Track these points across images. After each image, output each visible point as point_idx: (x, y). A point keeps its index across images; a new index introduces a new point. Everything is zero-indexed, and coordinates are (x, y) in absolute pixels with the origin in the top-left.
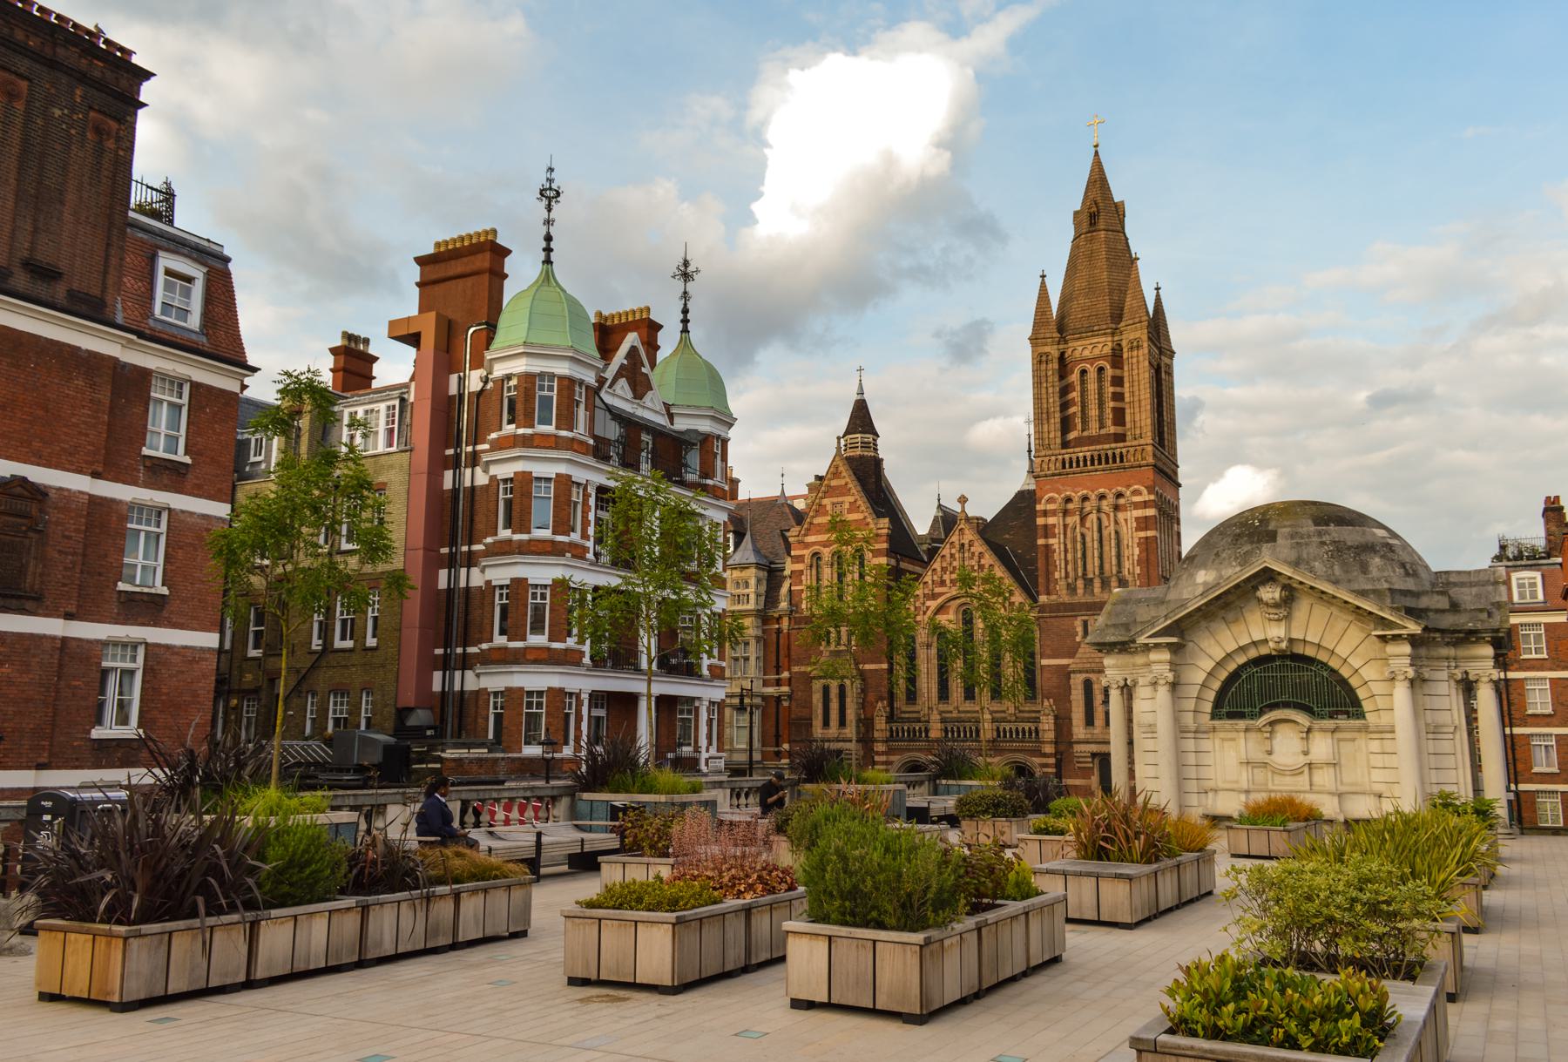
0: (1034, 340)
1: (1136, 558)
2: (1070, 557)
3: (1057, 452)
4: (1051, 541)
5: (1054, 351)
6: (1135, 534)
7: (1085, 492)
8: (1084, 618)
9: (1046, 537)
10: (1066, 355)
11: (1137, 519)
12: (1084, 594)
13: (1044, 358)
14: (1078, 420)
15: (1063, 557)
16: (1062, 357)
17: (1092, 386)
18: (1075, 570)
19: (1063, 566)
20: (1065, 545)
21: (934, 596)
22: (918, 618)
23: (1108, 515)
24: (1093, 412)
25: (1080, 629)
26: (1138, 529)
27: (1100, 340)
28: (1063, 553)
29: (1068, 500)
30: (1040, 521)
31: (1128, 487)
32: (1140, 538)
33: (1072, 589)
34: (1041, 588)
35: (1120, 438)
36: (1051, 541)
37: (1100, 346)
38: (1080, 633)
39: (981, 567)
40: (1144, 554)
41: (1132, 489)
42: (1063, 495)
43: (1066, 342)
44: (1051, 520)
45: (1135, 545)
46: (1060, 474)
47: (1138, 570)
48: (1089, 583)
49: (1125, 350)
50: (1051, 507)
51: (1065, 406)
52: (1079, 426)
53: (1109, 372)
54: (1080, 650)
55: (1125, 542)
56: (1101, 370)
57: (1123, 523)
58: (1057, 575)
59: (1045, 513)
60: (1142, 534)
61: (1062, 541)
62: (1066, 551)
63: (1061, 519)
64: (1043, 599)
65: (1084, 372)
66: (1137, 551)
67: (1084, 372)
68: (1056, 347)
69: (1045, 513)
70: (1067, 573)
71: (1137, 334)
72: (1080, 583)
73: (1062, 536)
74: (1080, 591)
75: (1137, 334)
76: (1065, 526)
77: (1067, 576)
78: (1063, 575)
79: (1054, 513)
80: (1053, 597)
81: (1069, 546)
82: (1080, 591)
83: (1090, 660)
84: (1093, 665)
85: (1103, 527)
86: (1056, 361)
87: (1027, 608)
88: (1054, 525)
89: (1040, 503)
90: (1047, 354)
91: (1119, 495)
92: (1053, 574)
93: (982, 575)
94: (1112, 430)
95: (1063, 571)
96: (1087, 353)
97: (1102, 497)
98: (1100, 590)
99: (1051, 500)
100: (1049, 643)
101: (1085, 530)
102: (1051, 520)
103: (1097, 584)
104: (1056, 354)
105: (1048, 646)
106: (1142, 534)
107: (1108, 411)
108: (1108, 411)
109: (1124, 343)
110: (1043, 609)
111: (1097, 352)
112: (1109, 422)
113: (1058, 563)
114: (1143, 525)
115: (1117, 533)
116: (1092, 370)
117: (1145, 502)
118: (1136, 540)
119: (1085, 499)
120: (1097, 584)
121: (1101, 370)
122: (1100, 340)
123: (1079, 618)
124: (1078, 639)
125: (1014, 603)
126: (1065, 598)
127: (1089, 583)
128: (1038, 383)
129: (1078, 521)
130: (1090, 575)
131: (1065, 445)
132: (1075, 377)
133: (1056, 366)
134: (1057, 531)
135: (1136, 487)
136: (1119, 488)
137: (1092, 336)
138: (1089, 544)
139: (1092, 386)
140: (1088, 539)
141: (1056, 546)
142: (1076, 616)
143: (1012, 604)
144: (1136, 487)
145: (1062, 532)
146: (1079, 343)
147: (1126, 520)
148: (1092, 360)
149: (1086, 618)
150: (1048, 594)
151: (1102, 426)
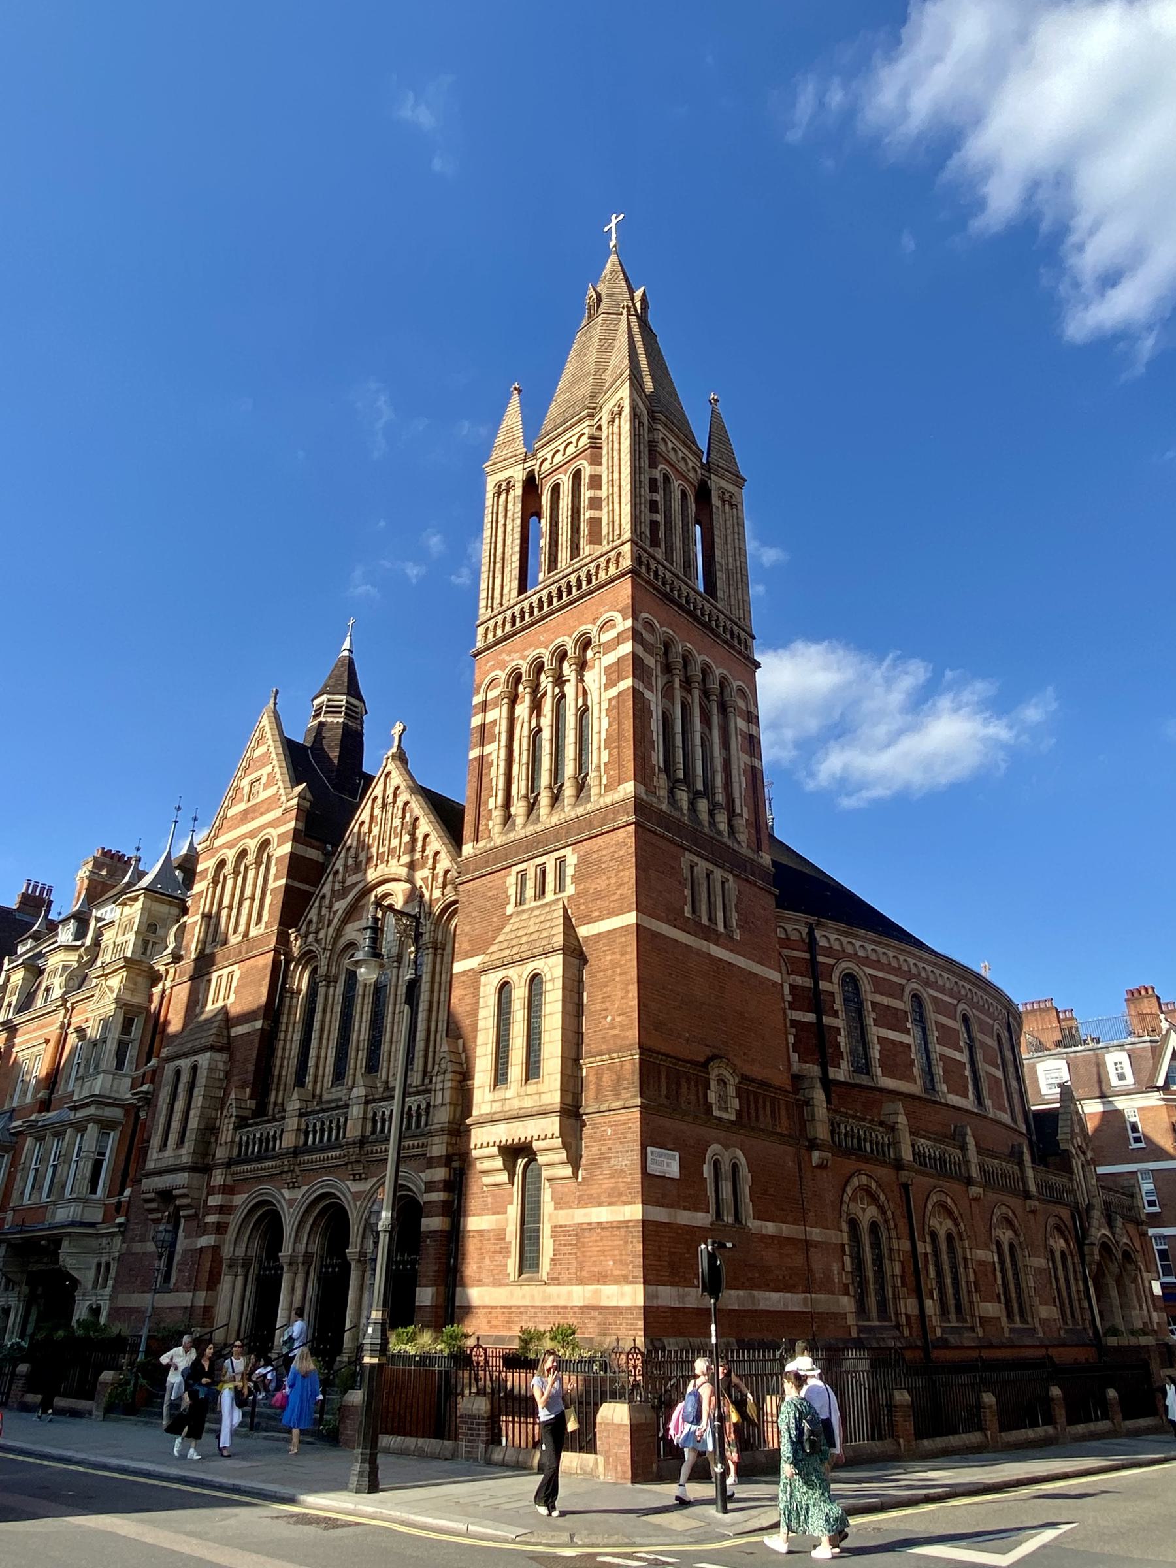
1: (603, 736)
7: (537, 651)
12: (525, 825)
21: (344, 892)
22: (321, 935)
25: (512, 891)
26: (610, 684)
32: (610, 700)
34: (468, 831)
40: (615, 727)
46: (506, 638)
54: (507, 929)
64: (468, 849)
88: (494, 722)
92: (487, 803)
114: (614, 676)
118: (605, 705)
121: (577, 475)
124: (510, 909)
141: (494, 756)
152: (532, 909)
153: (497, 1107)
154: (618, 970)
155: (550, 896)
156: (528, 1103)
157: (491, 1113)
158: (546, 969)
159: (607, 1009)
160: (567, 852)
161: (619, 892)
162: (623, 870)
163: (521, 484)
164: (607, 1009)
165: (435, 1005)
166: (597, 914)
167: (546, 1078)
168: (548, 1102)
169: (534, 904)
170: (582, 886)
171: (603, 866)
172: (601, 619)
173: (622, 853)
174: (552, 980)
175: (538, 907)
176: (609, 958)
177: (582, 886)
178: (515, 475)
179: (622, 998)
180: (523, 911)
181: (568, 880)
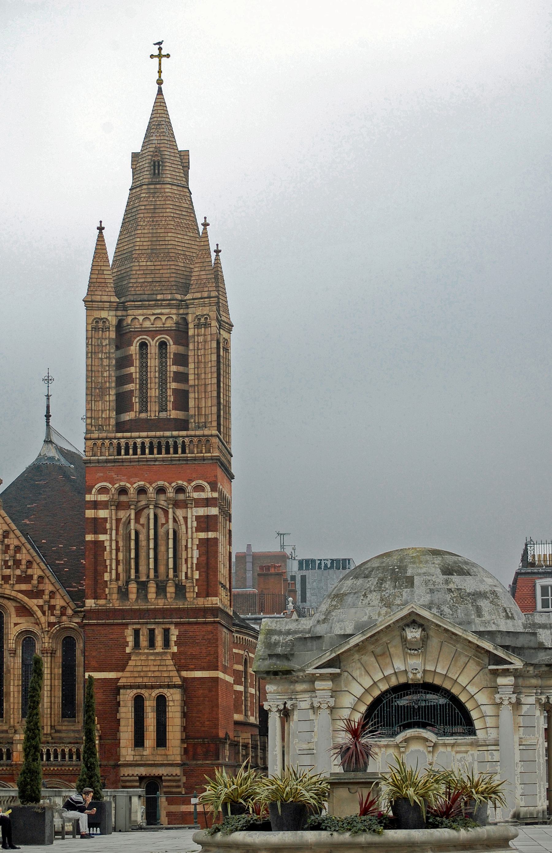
0: (89, 304)
1: (195, 561)
2: (121, 556)
3: (113, 435)
4: (102, 537)
5: (111, 317)
6: (195, 535)
7: (142, 483)
8: (135, 627)
9: (95, 533)
10: (125, 323)
11: (198, 518)
13: (101, 325)
14: (135, 400)
15: (114, 557)
16: (119, 326)
17: (153, 362)
18: (128, 571)
19: (114, 567)
20: (117, 542)
23: (166, 512)
24: (153, 392)
25: (130, 639)
26: (198, 530)
27: (164, 311)
28: (114, 552)
29: (123, 491)
30: (90, 513)
31: (190, 481)
33: (124, 593)
35: (183, 425)
36: (102, 537)
37: (164, 318)
38: (131, 644)
39: (17, 563)
40: (204, 558)
41: (193, 484)
42: (117, 486)
43: (125, 309)
44: (103, 513)
45: (195, 547)
47: (197, 576)
48: (143, 586)
49: (191, 326)
50: (103, 498)
51: (122, 380)
52: (137, 407)
53: (172, 348)
54: (130, 663)
55: (184, 543)
56: (163, 345)
57: (182, 521)
58: (106, 577)
59: (96, 505)
60: (202, 535)
61: (114, 538)
62: (118, 550)
63: (113, 512)
64: (90, 603)
65: (143, 345)
66: (196, 553)
67: (143, 345)
68: (113, 313)
69: (96, 505)
70: (118, 574)
71: (206, 311)
72: (133, 587)
73: (114, 532)
74: (133, 596)
75: (206, 311)
76: (118, 520)
77: (118, 578)
78: (114, 576)
79: (104, 505)
80: (102, 602)
81: (121, 544)
82: (133, 596)
83: (142, 674)
84: (145, 680)
85: (159, 524)
86: (113, 329)
87: (69, 612)
88: (105, 519)
89: (90, 493)
90: (104, 320)
91: (180, 490)
93: (18, 572)
94: (174, 414)
95: (114, 572)
96: (147, 324)
97: (161, 490)
98: (154, 596)
99: (103, 490)
100: (94, 654)
101: (139, 527)
102: (103, 513)
103: (152, 588)
104: (113, 321)
105: (94, 657)
106: (202, 535)
107: (170, 392)
108: (170, 392)
109: (190, 318)
110: (89, 614)
111: (159, 324)
112: (170, 406)
113: (108, 562)
114: (204, 525)
115: (175, 532)
116: (153, 343)
117: (207, 499)
118: (196, 542)
119: (142, 491)
120: (152, 588)
122: (164, 311)
123: (130, 627)
124: (128, 650)
125: (54, 606)
126: (116, 603)
127: (143, 586)
128: (91, 354)
129: (133, 516)
130: (143, 579)
131: (120, 427)
132: (134, 349)
133: (113, 335)
134: (108, 526)
135: (200, 482)
136: (180, 482)
137: (155, 305)
138: (143, 543)
139: (153, 362)
140: (142, 537)
141: (107, 544)
142: (127, 624)
143: (52, 608)
144: (200, 482)
145: (114, 527)
146: (140, 312)
147: (186, 519)
148: (153, 333)
149: (138, 626)
150: (96, 598)
151: (163, 409)
152: (148, 654)
153: (137, 758)
154: (207, 699)
155: (159, 650)
156: (159, 759)
157: (133, 761)
158: (168, 694)
159: (199, 717)
160: (172, 627)
161: (208, 658)
162: (209, 647)
163: (114, 329)
164: (199, 717)
165: (53, 687)
166: (193, 667)
167: (171, 749)
168: (173, 759)
169: (146, 651)
170: (182, 649)
171: (197, 641)
172: (194, 483)
173: (210, 637)
174: (173, 701)
175: (152, 654)
176: (201, 691)
177: (182, 649)
178: (109, 318)
179: (209, 713)
180: (140, 654)
181: (172, 643)
